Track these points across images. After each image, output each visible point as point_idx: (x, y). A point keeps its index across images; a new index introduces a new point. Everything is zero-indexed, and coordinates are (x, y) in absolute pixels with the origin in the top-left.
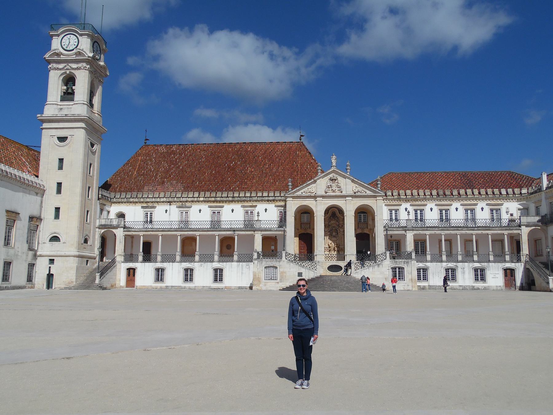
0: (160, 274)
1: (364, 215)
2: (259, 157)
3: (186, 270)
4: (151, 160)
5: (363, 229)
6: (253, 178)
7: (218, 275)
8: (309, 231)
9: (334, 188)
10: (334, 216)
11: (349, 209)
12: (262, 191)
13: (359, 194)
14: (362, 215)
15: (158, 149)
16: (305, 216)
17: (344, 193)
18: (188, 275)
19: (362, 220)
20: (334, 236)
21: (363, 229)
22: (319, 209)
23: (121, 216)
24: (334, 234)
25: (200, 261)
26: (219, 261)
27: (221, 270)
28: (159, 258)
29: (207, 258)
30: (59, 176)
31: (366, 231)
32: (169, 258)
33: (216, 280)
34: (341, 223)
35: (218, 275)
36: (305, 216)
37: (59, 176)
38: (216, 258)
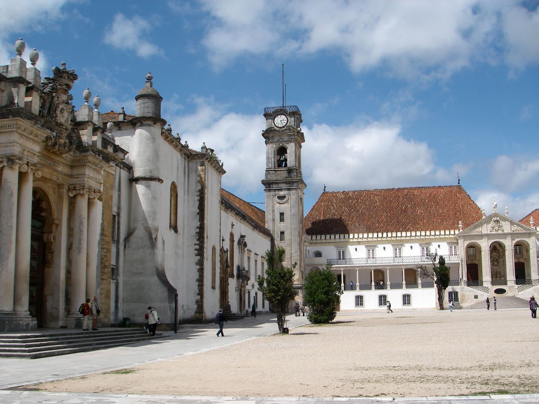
0: (359, 300)
1: (521, 249)
2: (425, 200)
3: (380, 297)
4: (333, 205)
5: (519, 259)
6: (424, 218)
7: (407, 299)
8: (475, 262)
9: (496, 228)
10: (497, 250)
11: (509, 244)
12: (435, 230)
13: (517, 232)
14: (518, 247)
15: (336, 195)
16: (473, 251)
17: (506, 231)
18: (383, 300)
19: (518, 252)
20: (496, 266)
21: (519, 259)
22: (485, 245)
23: (318, 254)
24: (496, 263)
25: (391, 288)
26: (407, 288)
27: (409, 296)
28: (358, 288)
29: (396, 286)
30: (282, 226)
31: (522, 260)
32: (366, 287)
33: (404, 303)
34: (501, 254)
35: (407, 299)
36: (473, 251)
37: (282, 226)
38: (404, 286)
